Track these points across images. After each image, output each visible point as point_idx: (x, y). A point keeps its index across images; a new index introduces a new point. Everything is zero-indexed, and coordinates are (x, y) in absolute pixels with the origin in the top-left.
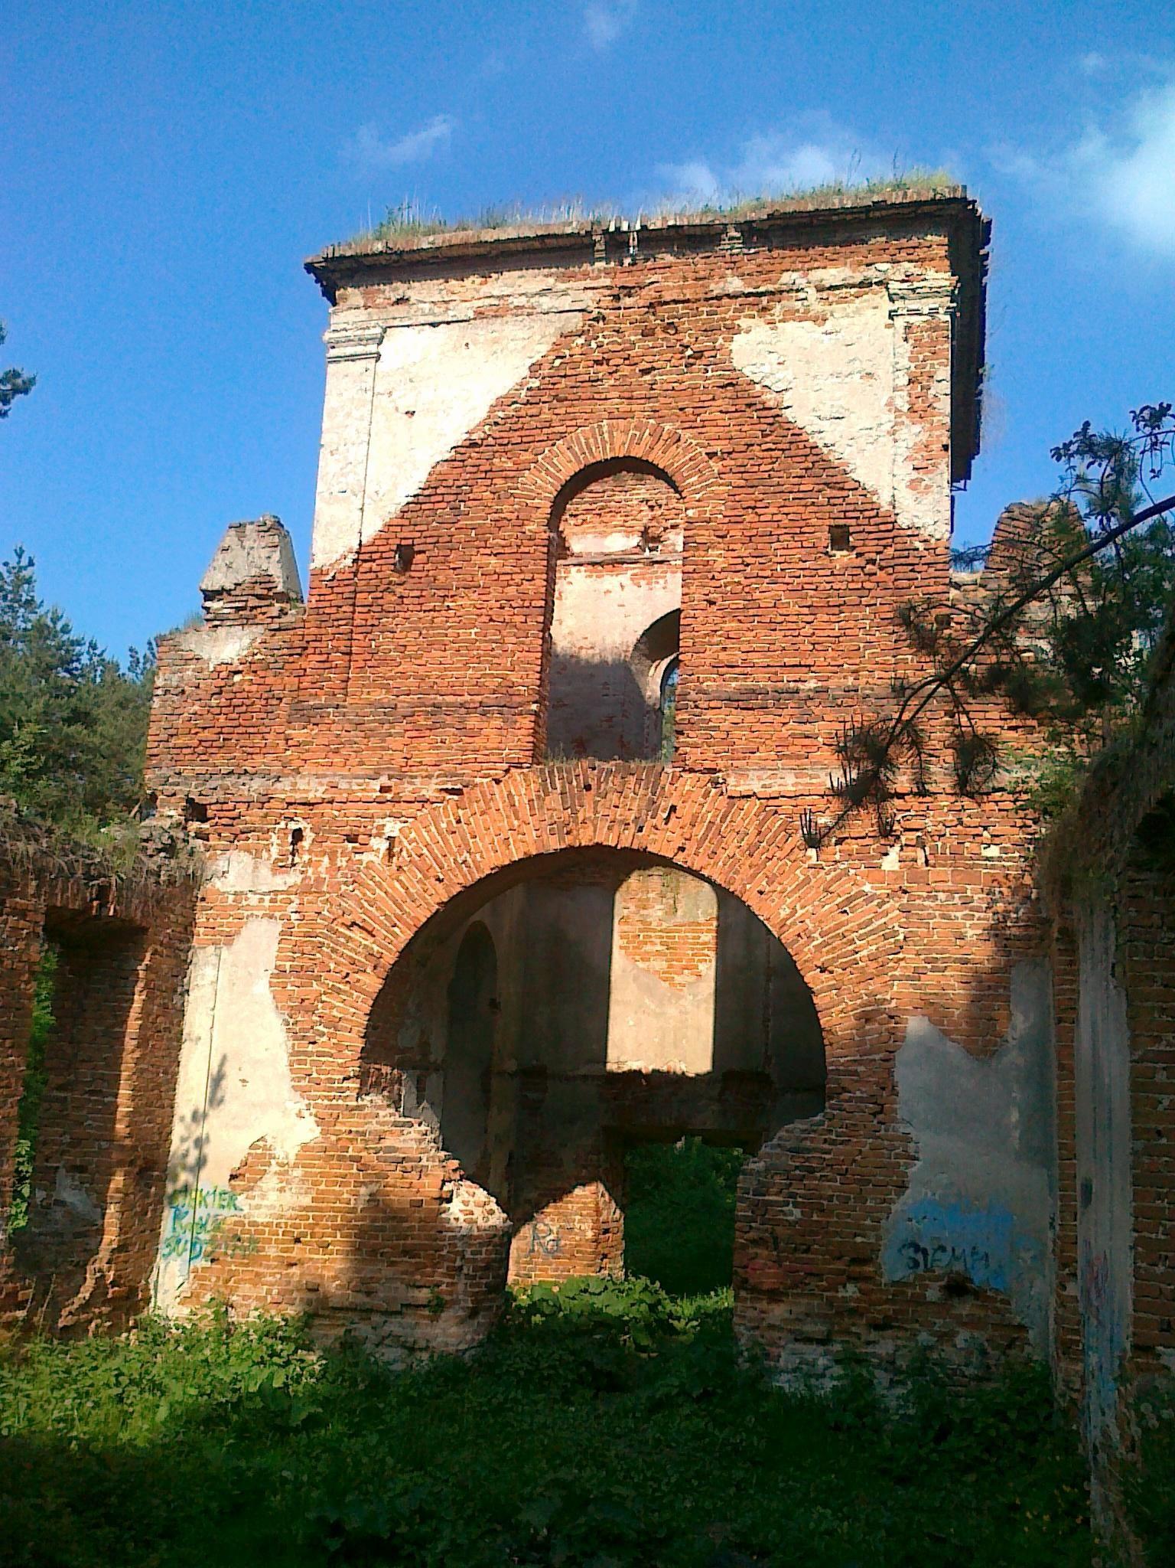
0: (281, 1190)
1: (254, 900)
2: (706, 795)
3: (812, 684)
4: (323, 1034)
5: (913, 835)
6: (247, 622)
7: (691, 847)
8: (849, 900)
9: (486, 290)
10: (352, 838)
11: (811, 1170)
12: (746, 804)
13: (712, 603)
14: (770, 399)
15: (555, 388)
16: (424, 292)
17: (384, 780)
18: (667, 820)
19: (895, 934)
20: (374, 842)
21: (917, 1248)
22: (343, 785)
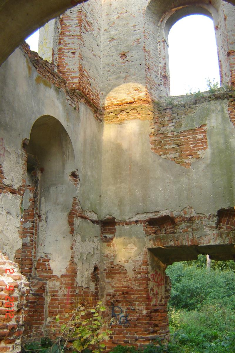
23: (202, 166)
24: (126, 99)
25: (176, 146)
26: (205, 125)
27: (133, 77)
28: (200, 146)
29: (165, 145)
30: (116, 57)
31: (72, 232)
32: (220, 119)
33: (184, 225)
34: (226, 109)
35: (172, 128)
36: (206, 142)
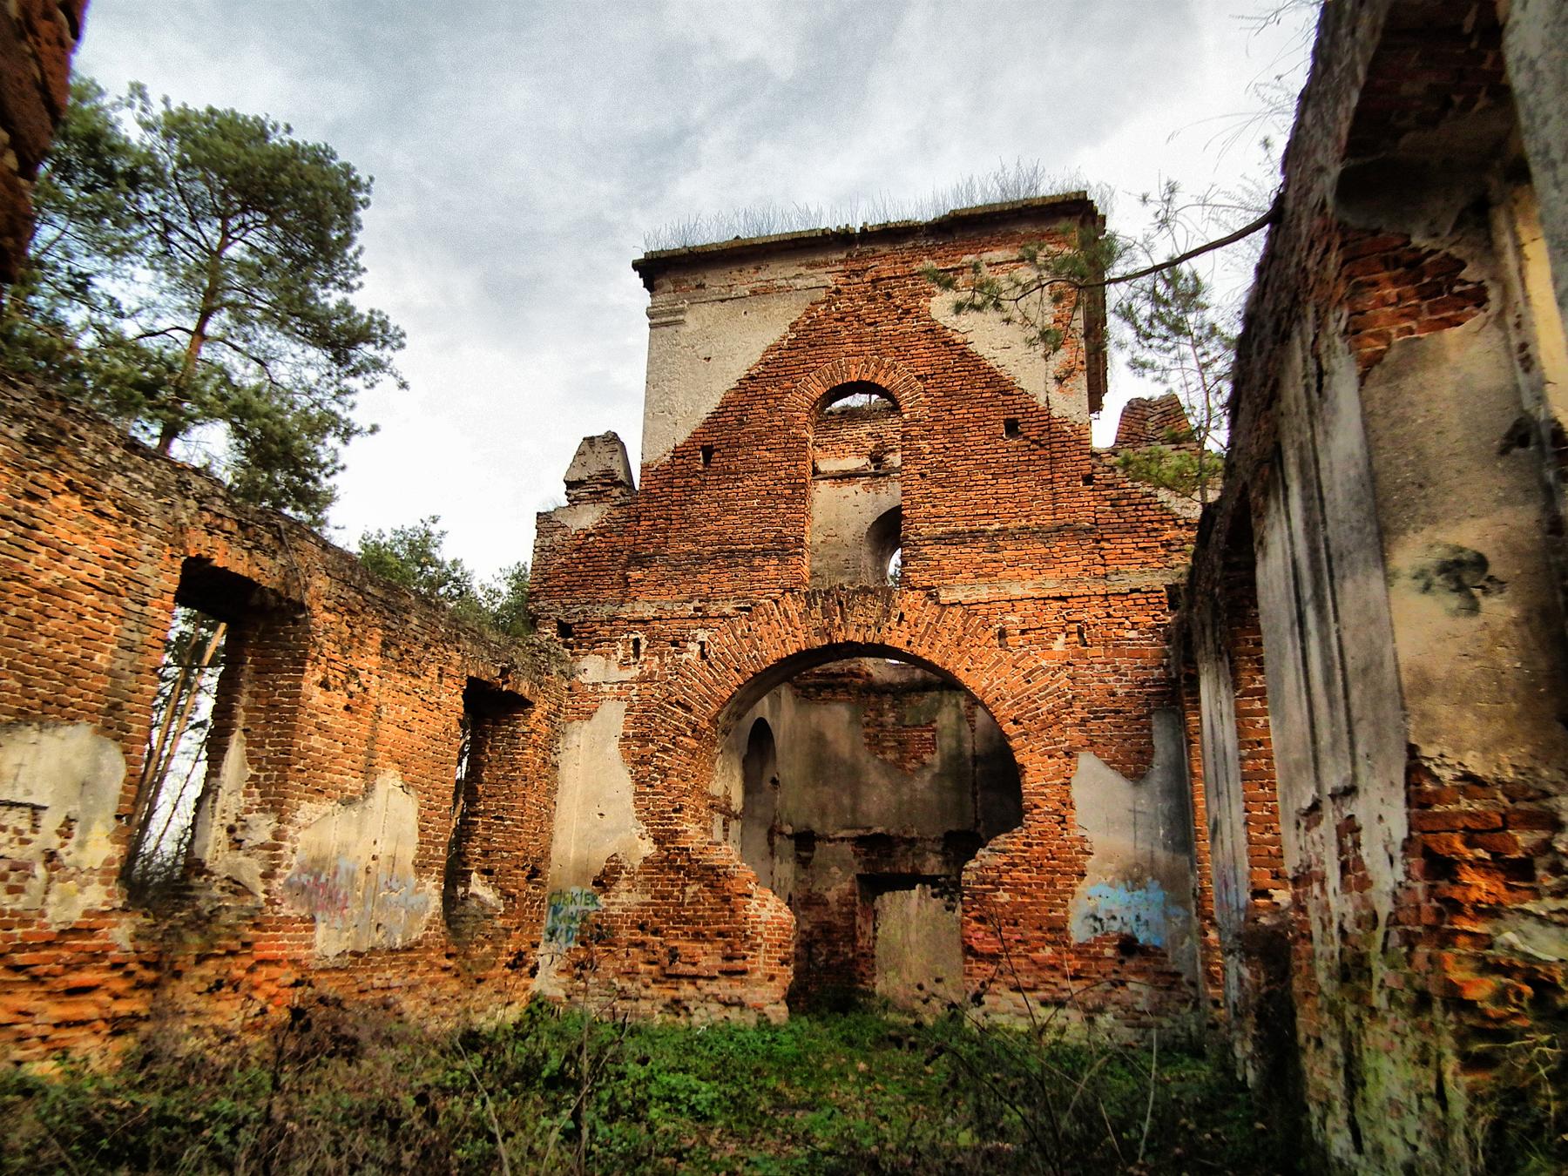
0: (629, 891)
1: (606, 688)
2: (924, 605)
3: (997, 526)
5: (1074, 627)
6: (600, 500)
8: (1031, 672)
9: (756, 277)
10: (675, 643)
11: (1015, 865)
12: (954, 610)
13: (923, 475)
14: (958, 338)
15: (807, 340)
16: (715, 281)
17: (696, 603)
18: (899, 623)
19: (1065, 694)
20: (690, 646)
21: (1096, 918)
22: (668, 607)
23: (928, 776)
31: (772, 854)
32: (953, 717)
33: (903, 847)
34: (962, 703)
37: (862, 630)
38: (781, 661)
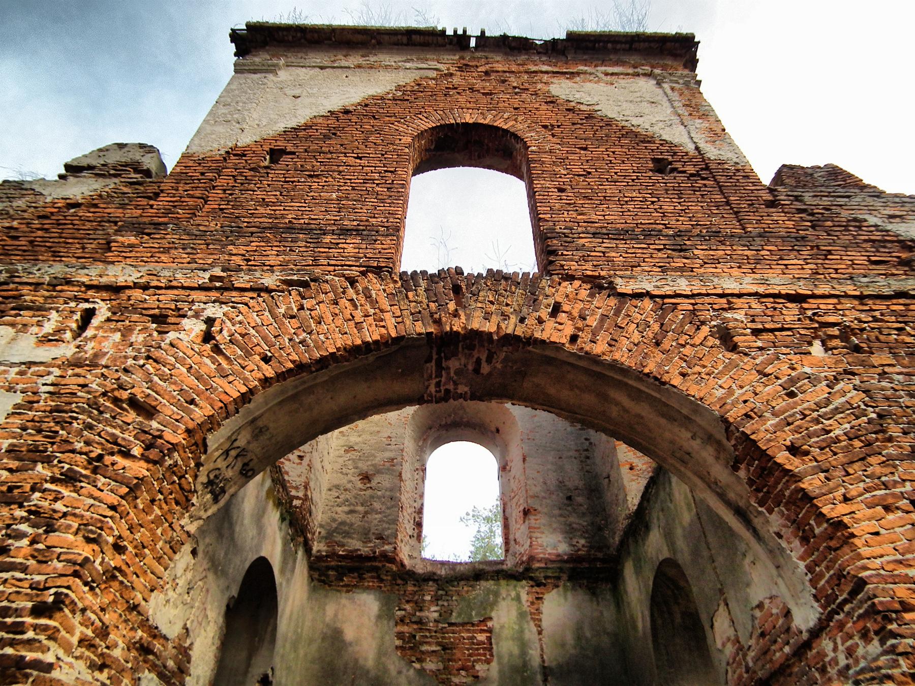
4: (20, 536)
7: (585, 336)
17: (218, 272)
24: (360, 550)
25: (438, 648)
26: (491, 619)
27: (376, 516)
28: (479, 655)
29: (422, 643)
30: (353, 479)
32: (514, 613)
34: (524, 597)
35: (436, 615)
36: (491, 649)
37: (495, 319)
38: (354, 351)
